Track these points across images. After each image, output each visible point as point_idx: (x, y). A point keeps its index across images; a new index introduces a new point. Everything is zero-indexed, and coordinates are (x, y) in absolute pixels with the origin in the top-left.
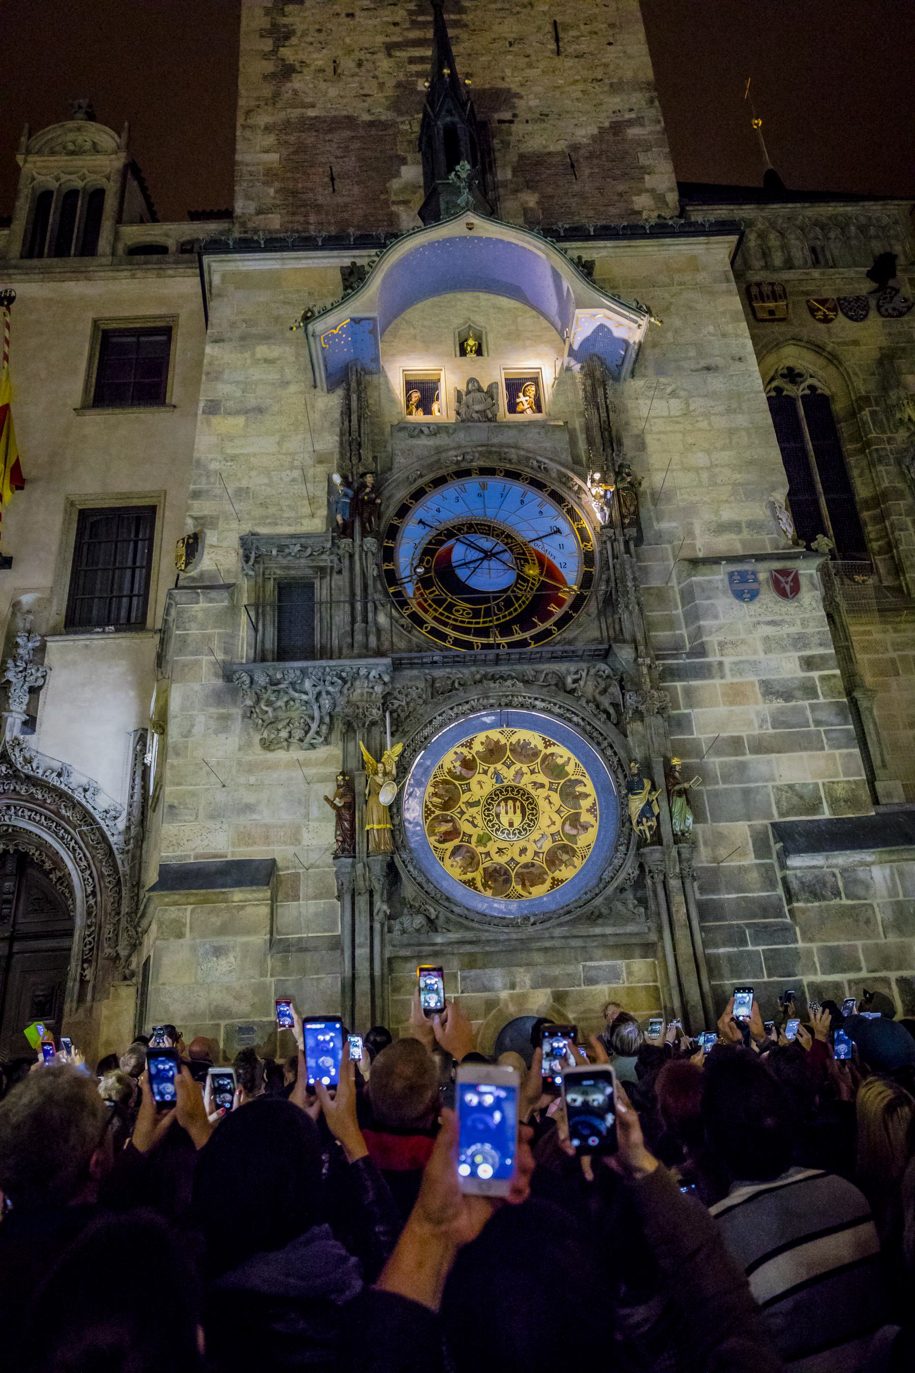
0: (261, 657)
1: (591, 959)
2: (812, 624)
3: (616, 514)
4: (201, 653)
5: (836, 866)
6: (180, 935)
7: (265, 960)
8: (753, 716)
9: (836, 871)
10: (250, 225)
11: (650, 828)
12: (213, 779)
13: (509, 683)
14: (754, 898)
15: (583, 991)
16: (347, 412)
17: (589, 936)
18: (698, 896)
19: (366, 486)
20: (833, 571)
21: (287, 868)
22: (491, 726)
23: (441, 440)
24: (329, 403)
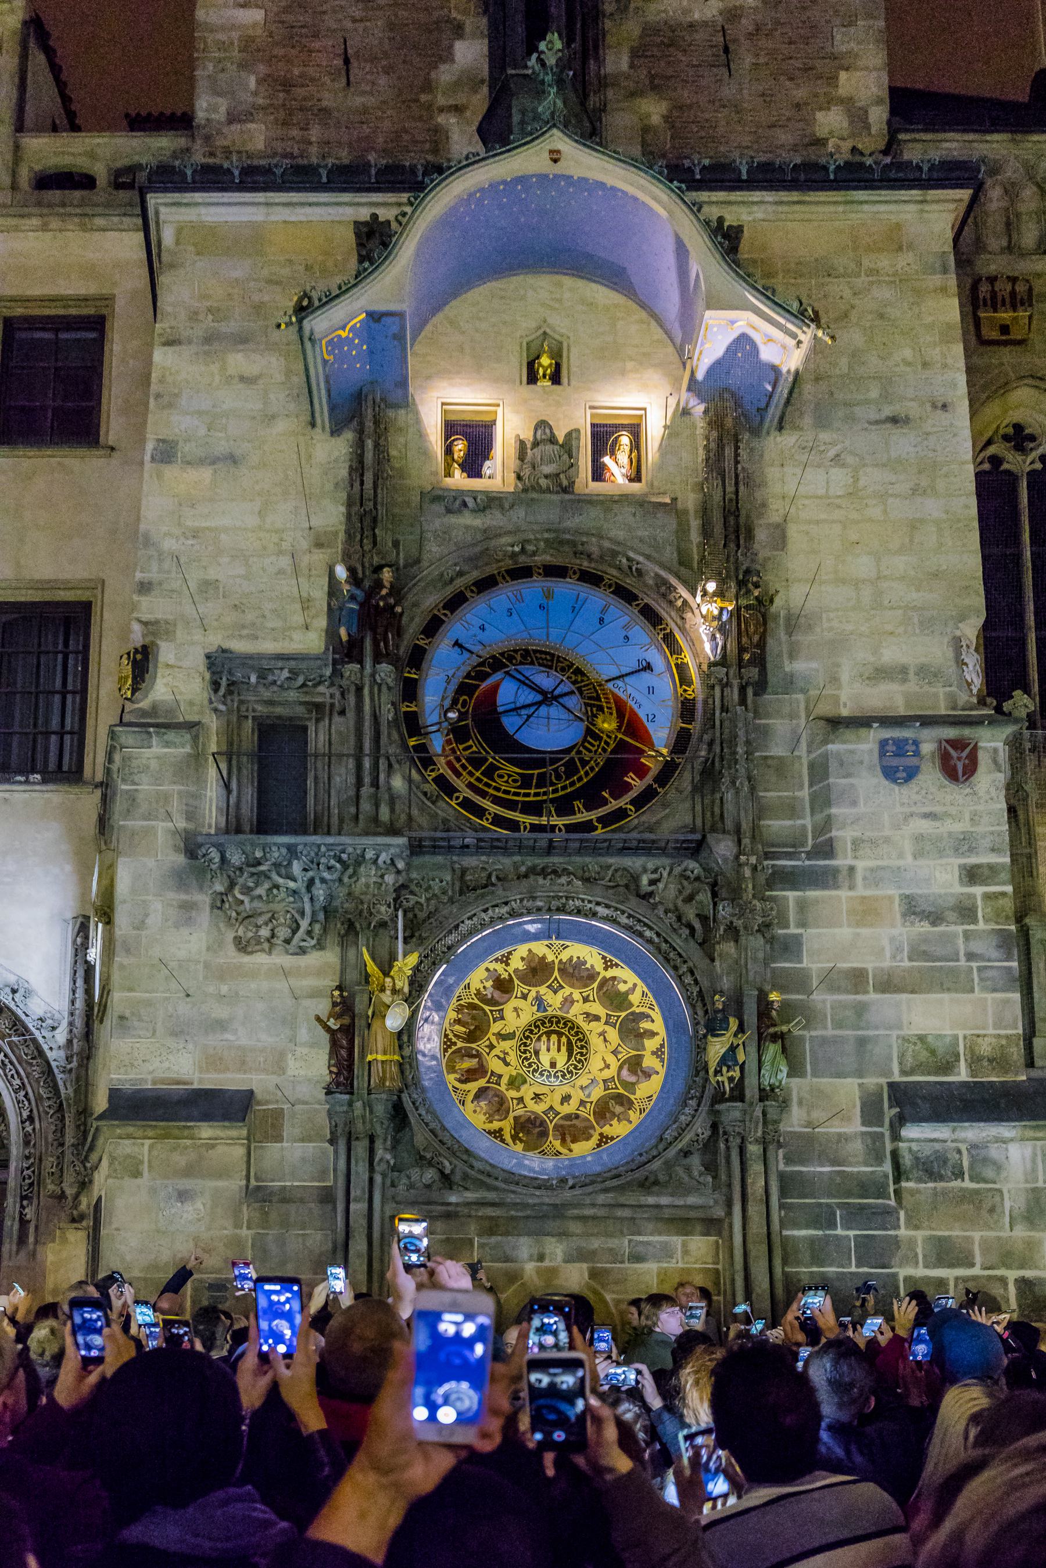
0: (234, 827)
1: (640, 1234)
2: (985, 819)
3: (732, 646)
4: (156, 818)
5: (964, 1141)
6: (137, 1174)
8: (885, 943)
9: (963, 1148)
10: (220, 142)
11: (731, 1079)
12: (174, 985)
13: (563, 880)
14: (852, 1173)
15: (626, 1269)
16: (358, 467)
17: (640, 1206)
18: (782, 1166)
19: (383, 586)
20: (1028, 745)
21: (267, 1102)
22: (536, 937)
23: (494, 519)
24: (332, 452)
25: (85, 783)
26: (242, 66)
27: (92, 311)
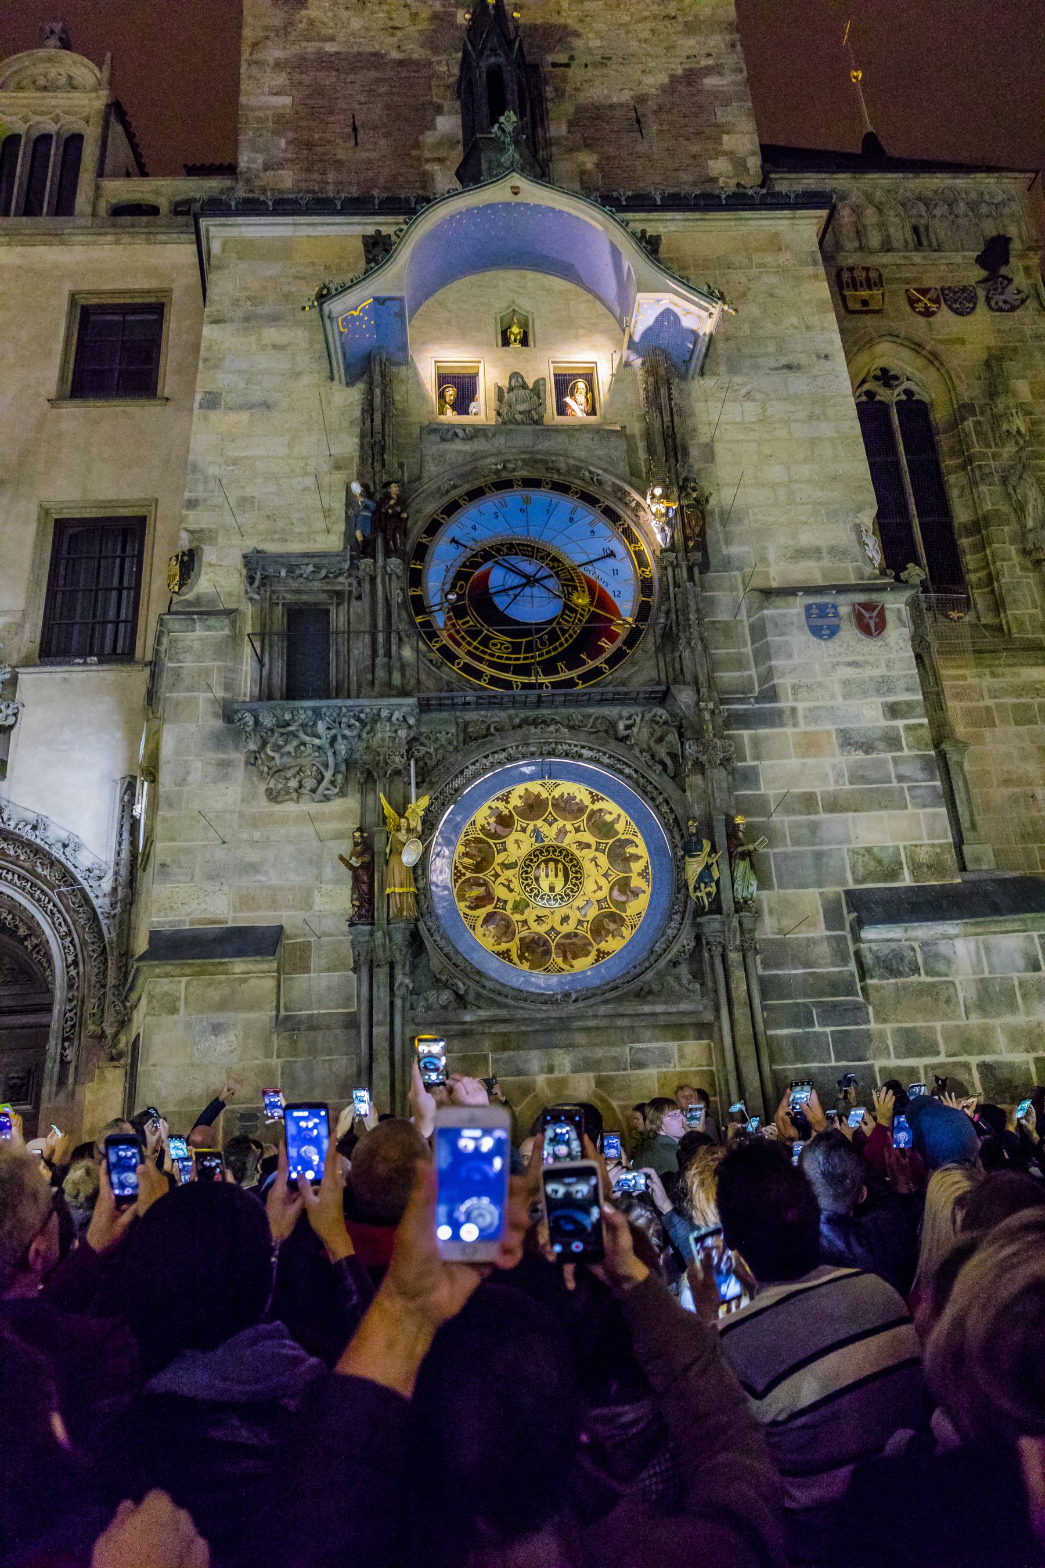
0: (266, 694)
3: (679, 536)
4: (198, 690)
5: (916, 939)
6: (173, 1010)
7: (271, 1041)
8: (828, 770)
9: (916, 945)
10: (258, 183)
11: (709, 894)
12: (211, 834)
13: (552, 728)
14: (822, 975)
16: (368, 409)
17: (638, 1015)
18: (760, 971)
20: (924, 606)
21: (296, 936)
22: (531, 778)
23: (481, 445)
24: (348, 399)
25: (137, 663)
26: (275, 133)
27: (154, 300)
